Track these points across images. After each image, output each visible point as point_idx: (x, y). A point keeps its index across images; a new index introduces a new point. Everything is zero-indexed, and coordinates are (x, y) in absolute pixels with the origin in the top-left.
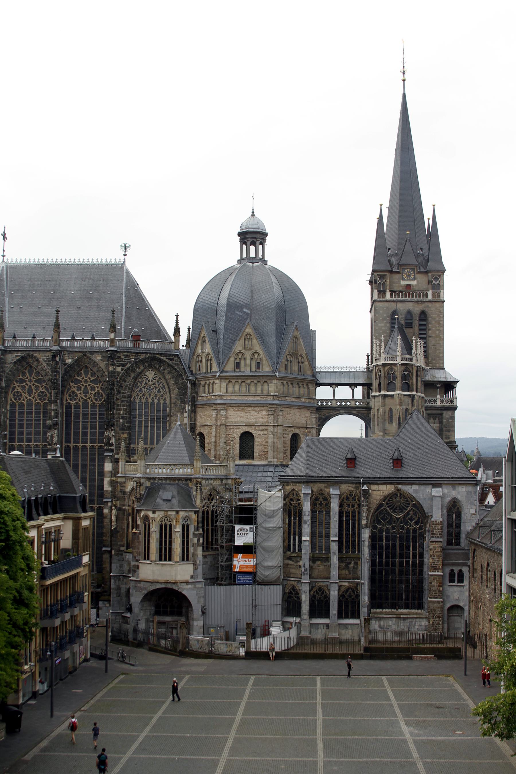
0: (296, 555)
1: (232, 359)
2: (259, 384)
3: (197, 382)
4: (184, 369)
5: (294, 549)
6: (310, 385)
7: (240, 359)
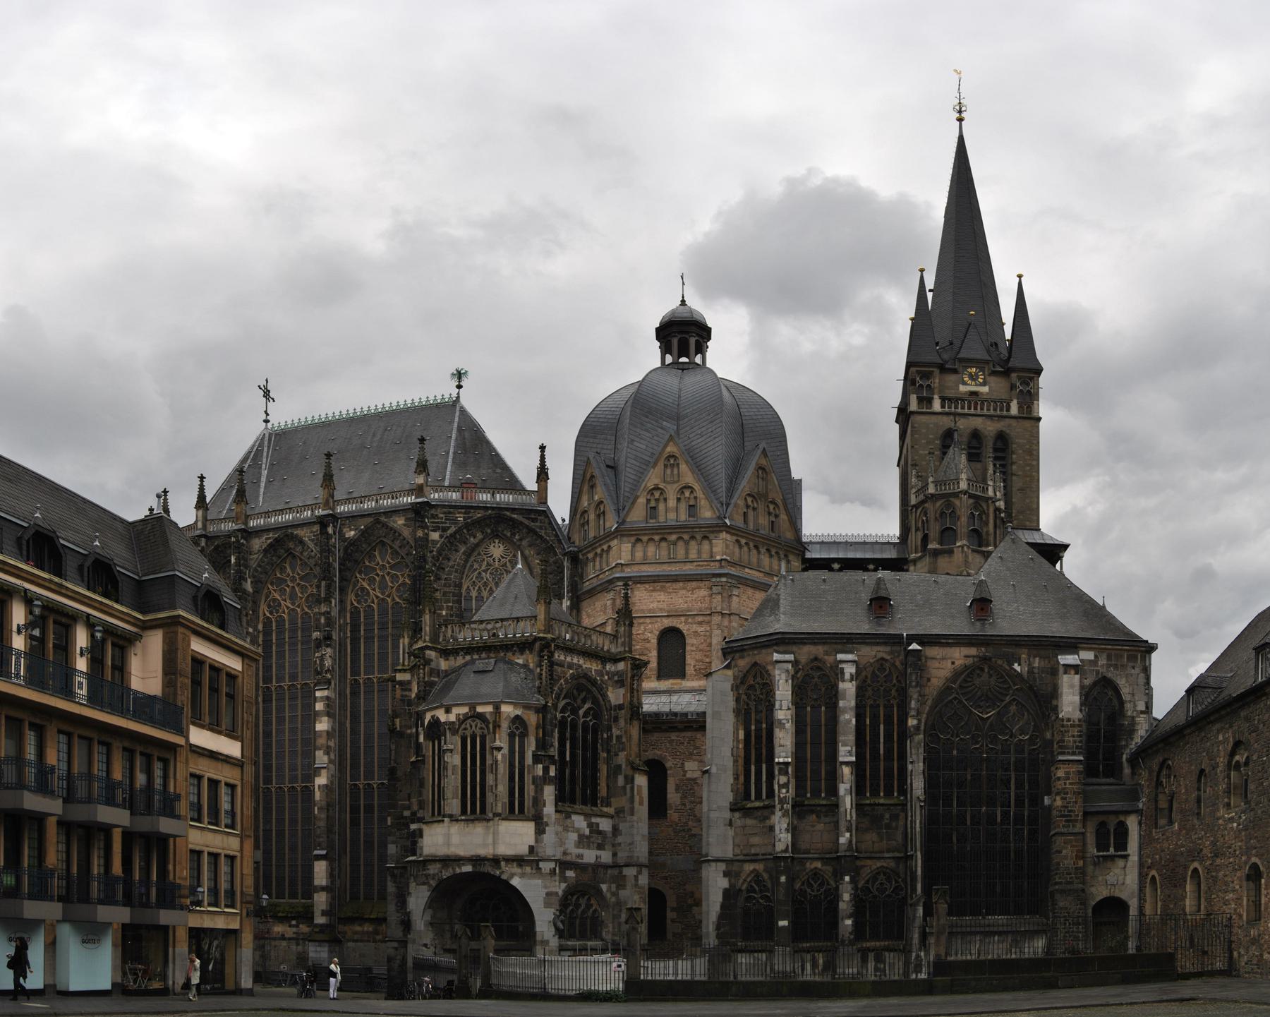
0: (762, 804)
1: (642, 500)
2: (693, 543)
3: (581, 557)
4: (557, 535)
5: (758, 797)
6: (791, 557)
7: (657, 500)
